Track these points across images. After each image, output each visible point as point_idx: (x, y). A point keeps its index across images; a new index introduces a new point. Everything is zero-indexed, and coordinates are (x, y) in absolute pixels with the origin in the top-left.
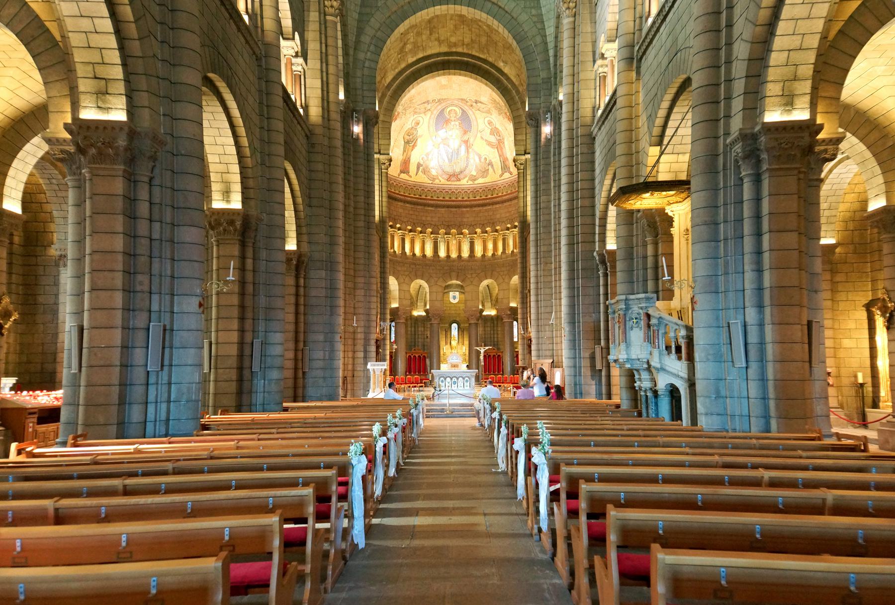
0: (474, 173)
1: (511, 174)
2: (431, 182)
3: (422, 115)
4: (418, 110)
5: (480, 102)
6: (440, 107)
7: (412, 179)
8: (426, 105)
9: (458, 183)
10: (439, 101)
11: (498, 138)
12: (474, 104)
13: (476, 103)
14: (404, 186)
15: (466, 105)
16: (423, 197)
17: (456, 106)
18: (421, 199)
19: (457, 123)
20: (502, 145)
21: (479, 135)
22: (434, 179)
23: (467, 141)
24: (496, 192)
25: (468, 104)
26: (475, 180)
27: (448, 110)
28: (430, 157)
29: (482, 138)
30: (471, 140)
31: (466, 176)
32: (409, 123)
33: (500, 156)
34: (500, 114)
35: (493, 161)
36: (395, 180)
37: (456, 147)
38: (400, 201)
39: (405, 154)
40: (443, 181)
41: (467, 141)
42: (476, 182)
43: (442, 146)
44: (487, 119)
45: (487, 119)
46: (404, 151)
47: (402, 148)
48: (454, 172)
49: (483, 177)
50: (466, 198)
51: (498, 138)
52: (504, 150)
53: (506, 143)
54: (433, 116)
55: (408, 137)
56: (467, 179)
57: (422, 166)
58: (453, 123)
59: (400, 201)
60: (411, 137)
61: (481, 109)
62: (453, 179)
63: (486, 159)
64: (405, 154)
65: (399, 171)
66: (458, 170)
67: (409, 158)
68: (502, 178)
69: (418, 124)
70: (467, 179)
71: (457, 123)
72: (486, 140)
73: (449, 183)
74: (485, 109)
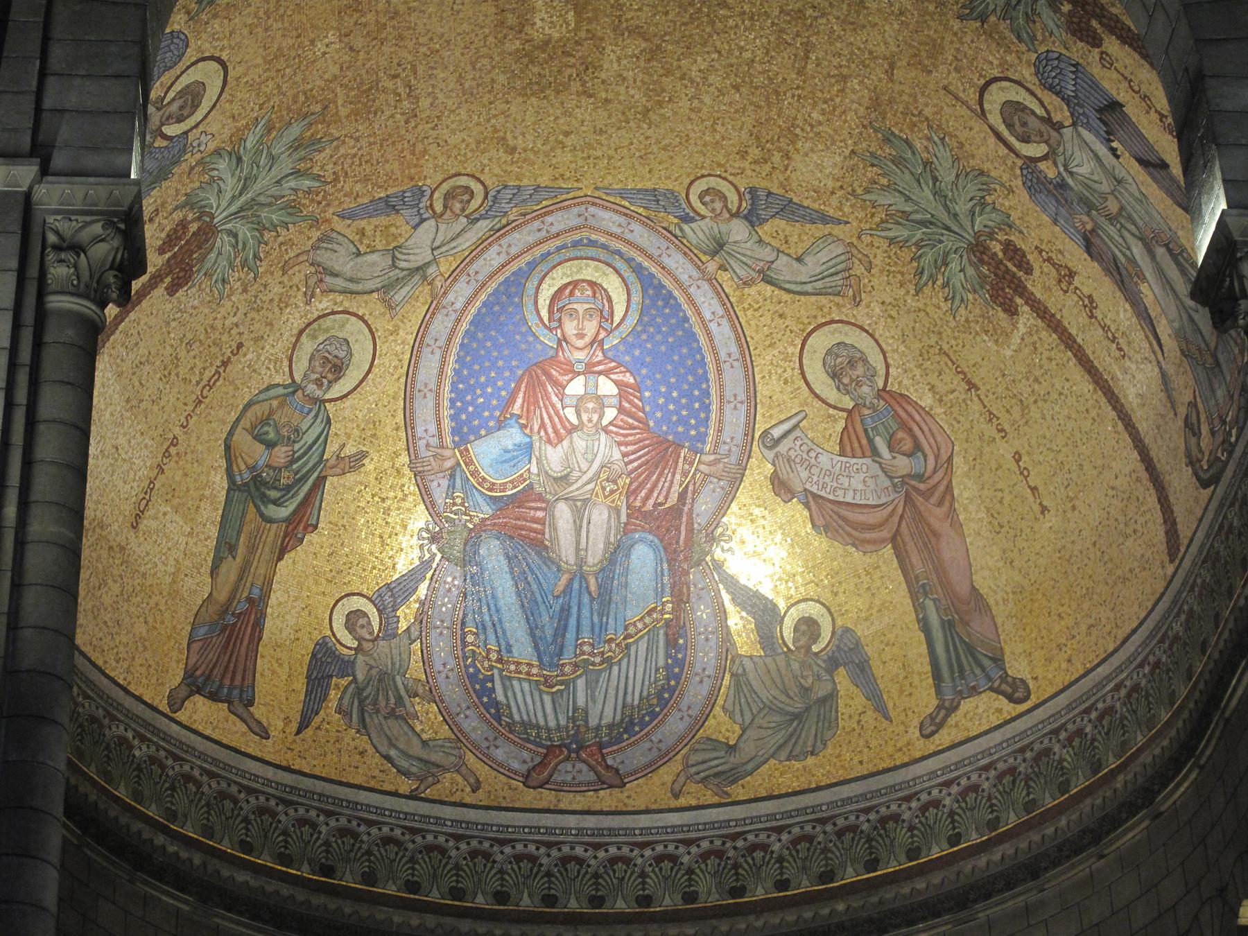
0: (721, 726)
1: (1015, 691)
2: (405, 786)
3: (370, 306)
4: (340, 260)
5: (789, 209)
6: (493, 257)
7: (267, 750)
8: (401, 223)
9: (607, 799)
10: (492, 199)
11: (903, 464)
12: (738, 231)
13: (752, 218)
14: (210, 787)
15: (678, 240)
16: (349, 880)
17: (607, 255)
18: (333, 891)
19: (607, 387)
20: (935, 515)
21: (760, 469)
22: (431, 771)
23: (676, 511)
24: (902, 835)
25: (697, 233)
26: (733, 775)
27: (558, 278)
28: (406, 616)
29: (781, 486)
30: (703, 506)
31: (665, 756)
32: (277, 346)
33: (917, 591)
34: (921, 280)
35: (862, 631)
36: (148, 732)
37: (596, 553)
38: (179, 878)
39: (230, 569)
40: (496, 785)
41: (676, 511)
42: (738, 792)
43: (492, 553)
44: (821, 342)
45: (821, 342)
46: (226, 547)
47: (211, 515)
48: (579, 717)
49: (792, 749)
50: (668, 902)
51: (903, 464)
52: (949, 551)
53: (965, 490)
54: (440, 326)
55: (252, 452)
56: (676, 766)
57: (346, 667)
58: (576, 387)
59: (179, 878)
60: (281, 454)
61: (784, 268)
62: (567, 771)
63: (808, 627)
64: (230, 569)
65: (175, 677)
66: (604, 712)
67: (256, 608)
68: (945, 737)
69: (338, 369)
70: (676, 766)
71: (607, 387)
72: (811, 500)
73: (546, 798)
74: (814, 264)
